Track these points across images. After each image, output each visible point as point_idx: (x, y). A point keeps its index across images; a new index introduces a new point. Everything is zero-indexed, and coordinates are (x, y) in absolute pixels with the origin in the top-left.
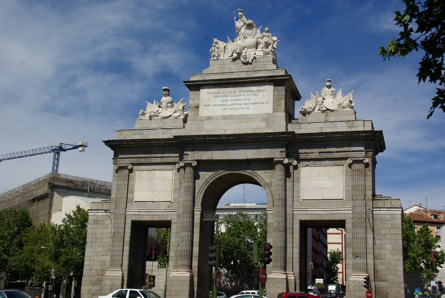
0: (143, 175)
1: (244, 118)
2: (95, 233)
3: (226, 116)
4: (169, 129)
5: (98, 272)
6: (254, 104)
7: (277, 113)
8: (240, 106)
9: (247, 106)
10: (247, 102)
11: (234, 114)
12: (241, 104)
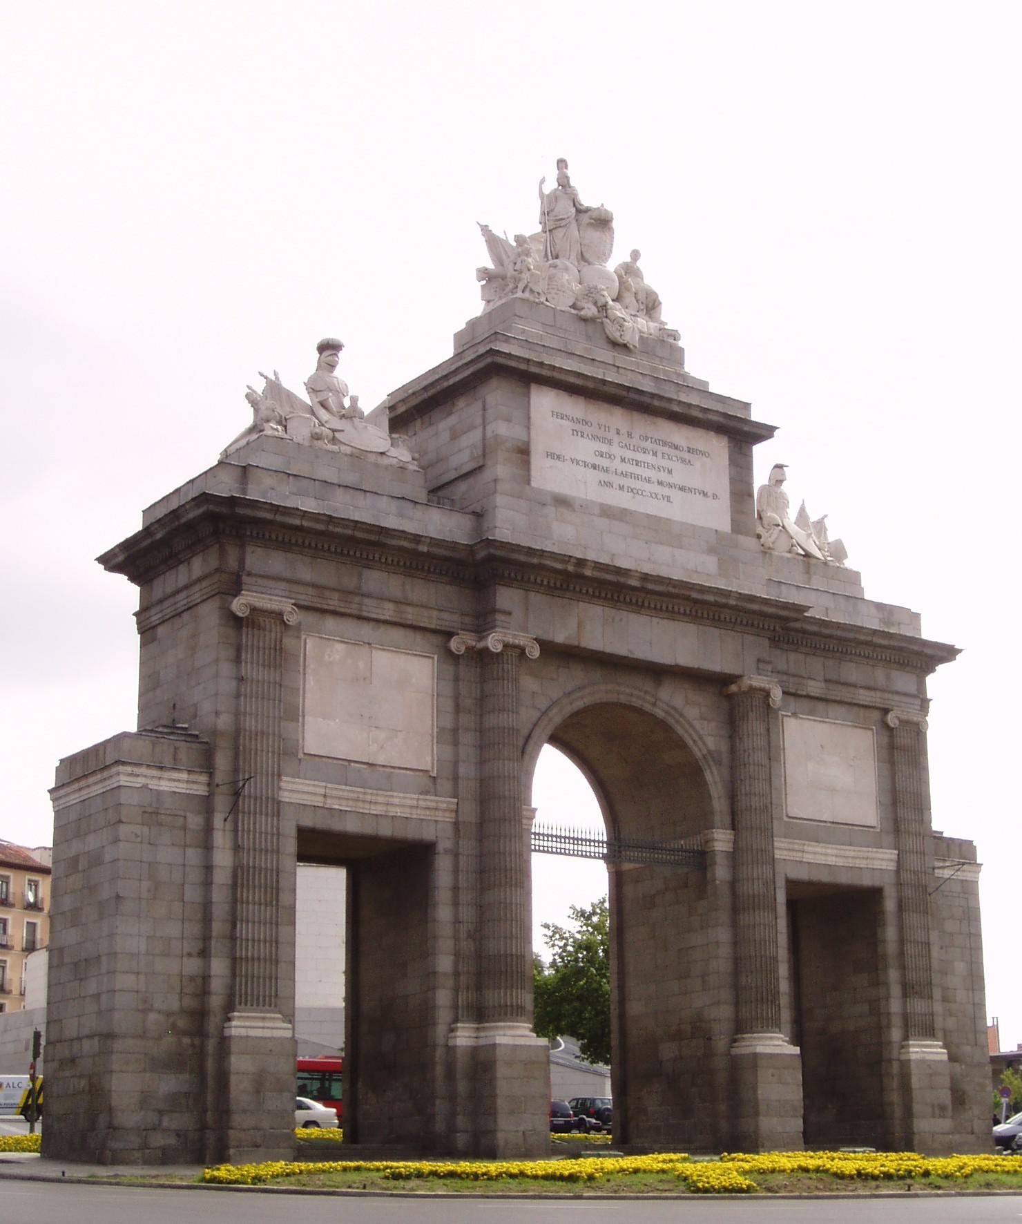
0: (330, 657)
1: (658, 529)
2: (150, 864)
3: (610, 507)
4: (418, 506)
5: (171, 1020)
6: (682, 489)
7: (740, 537)
8: (647, 487)
9: (666, 491)
10: (664, 477)
11: (633, 509)
12: (649, 481)
